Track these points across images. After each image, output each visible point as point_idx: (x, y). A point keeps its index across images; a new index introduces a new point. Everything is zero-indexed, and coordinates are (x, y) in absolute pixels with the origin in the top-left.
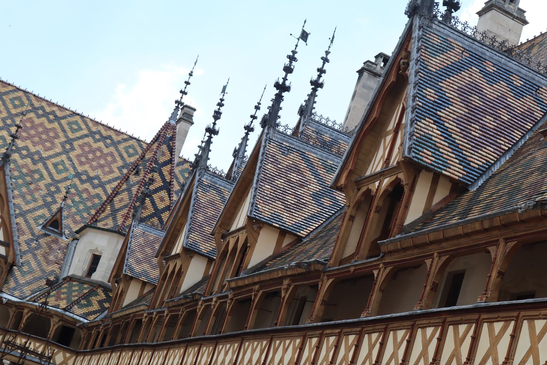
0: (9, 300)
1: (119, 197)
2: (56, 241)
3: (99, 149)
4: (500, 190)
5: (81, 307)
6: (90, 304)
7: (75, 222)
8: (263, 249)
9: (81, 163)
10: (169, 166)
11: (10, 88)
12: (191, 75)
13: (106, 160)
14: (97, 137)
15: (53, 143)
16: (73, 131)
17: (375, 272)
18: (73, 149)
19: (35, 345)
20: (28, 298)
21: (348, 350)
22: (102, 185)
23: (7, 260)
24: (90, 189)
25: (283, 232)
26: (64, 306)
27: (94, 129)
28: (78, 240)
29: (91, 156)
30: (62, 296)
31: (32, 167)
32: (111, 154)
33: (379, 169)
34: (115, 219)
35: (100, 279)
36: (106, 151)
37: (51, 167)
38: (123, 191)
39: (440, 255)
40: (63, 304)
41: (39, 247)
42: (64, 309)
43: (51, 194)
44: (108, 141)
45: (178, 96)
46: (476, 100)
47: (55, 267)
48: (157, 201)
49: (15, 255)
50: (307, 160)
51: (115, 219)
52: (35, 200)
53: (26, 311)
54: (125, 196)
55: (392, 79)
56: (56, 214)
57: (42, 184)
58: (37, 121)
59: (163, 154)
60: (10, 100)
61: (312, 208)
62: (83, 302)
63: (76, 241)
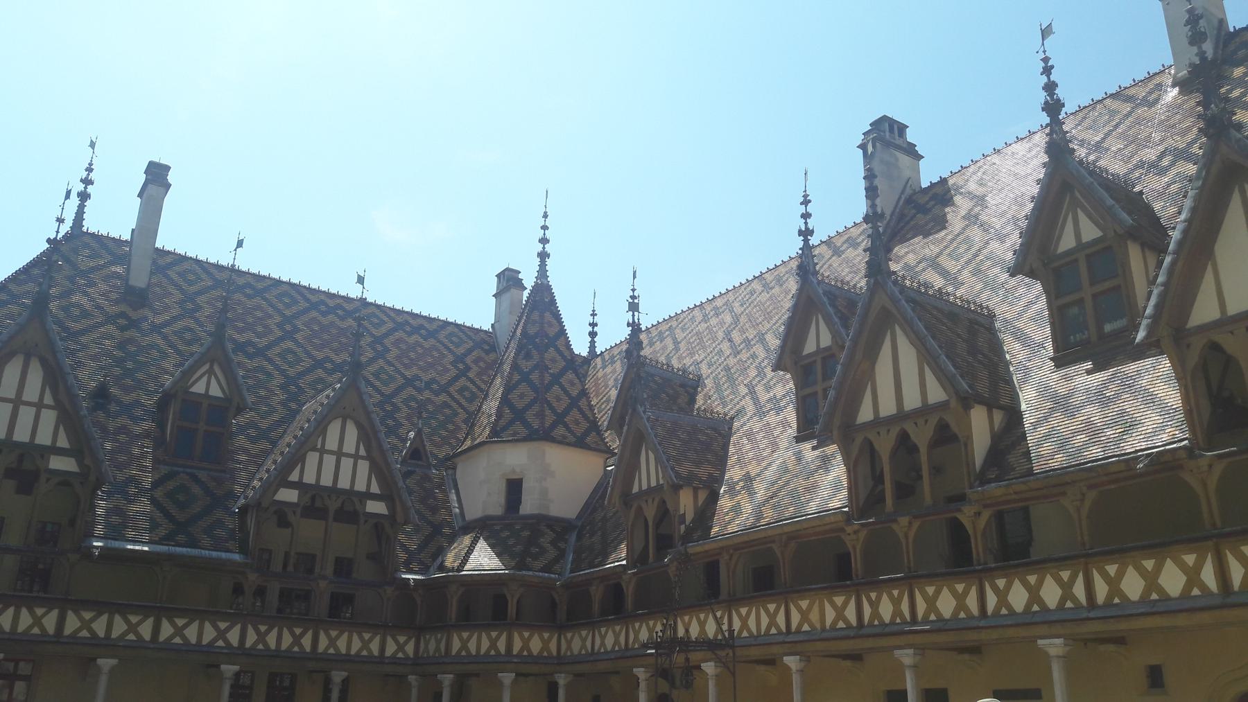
1: (517, 392)
2: (426, 478)
3: (417, 344)
9: (406, 367)
11: (269, 283)
12: (545, 216)
19: (489, 637)
27: (399, 319)
28: (454, 469)
29: (412, 355)
34: (526, 424)
35: (536, 512)
44: (423, 332)
48: (567, 386)
51: (526, 424)
54: (523, 388)
59: (551, 325)
62: (534, 550)
63: (450, 472)
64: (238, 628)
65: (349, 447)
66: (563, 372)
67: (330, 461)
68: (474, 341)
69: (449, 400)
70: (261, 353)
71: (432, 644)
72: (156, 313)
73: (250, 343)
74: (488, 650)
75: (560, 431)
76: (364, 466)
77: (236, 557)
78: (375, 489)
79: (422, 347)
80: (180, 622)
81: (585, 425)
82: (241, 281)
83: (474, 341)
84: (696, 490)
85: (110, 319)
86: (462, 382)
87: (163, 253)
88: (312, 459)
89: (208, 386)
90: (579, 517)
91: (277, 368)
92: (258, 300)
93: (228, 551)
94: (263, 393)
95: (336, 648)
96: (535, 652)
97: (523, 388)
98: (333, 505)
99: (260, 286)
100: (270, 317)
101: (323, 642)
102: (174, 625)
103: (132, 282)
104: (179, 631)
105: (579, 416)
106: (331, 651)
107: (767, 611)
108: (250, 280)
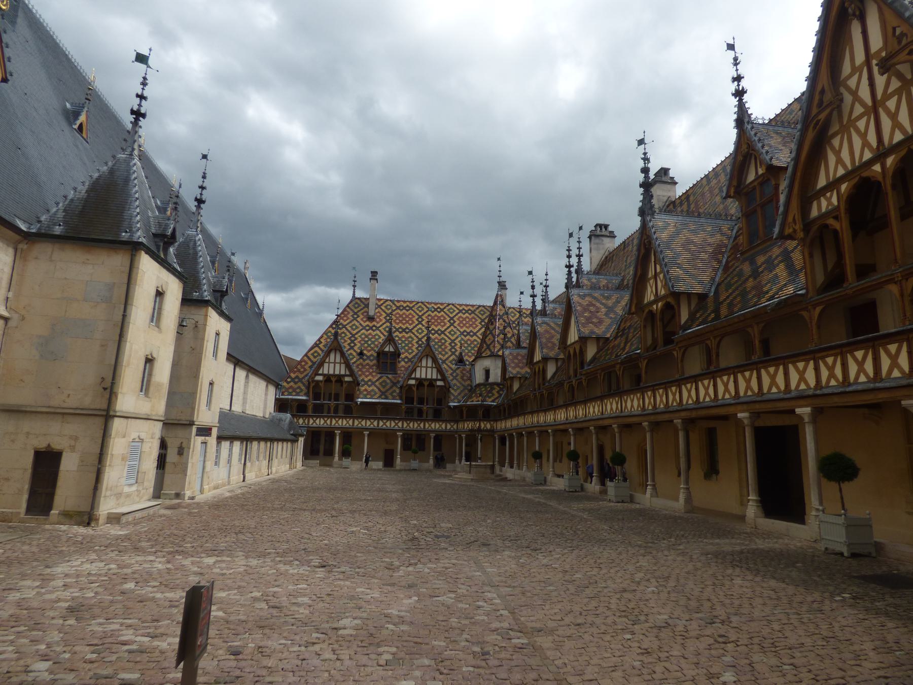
2: (464, 370)
4: (731, 294)
8: (591, 351)
9: (462, 327)
17: (675, 353)
21: (674, 395)
22: (475, 334)
25: (598, 339)
31: (440, 338)
33: (652, 298)
34: (490, 350)
39: (715, 338)
41: (457, 375)
43: (453, 347)
45: (498, 279)
46: (693, 248)
47: (468, 382)
50: (595, 298)
51: (490, 350)
52: (447, 353)
54: (490, 336)
55: (643, 251)
57: (447, 344)
58: (433, 315)
61: (608, 321)
65: (430, 364)
67: (424, 370)
70: (411, 331)
71: (461, 426)
77: (399, 401)
85: (364, 328)
87: (380, 300)
88: (418, 370)
89: (389, 348)
97: (490, 336)
98: (426, 383)
104: (385, 424)
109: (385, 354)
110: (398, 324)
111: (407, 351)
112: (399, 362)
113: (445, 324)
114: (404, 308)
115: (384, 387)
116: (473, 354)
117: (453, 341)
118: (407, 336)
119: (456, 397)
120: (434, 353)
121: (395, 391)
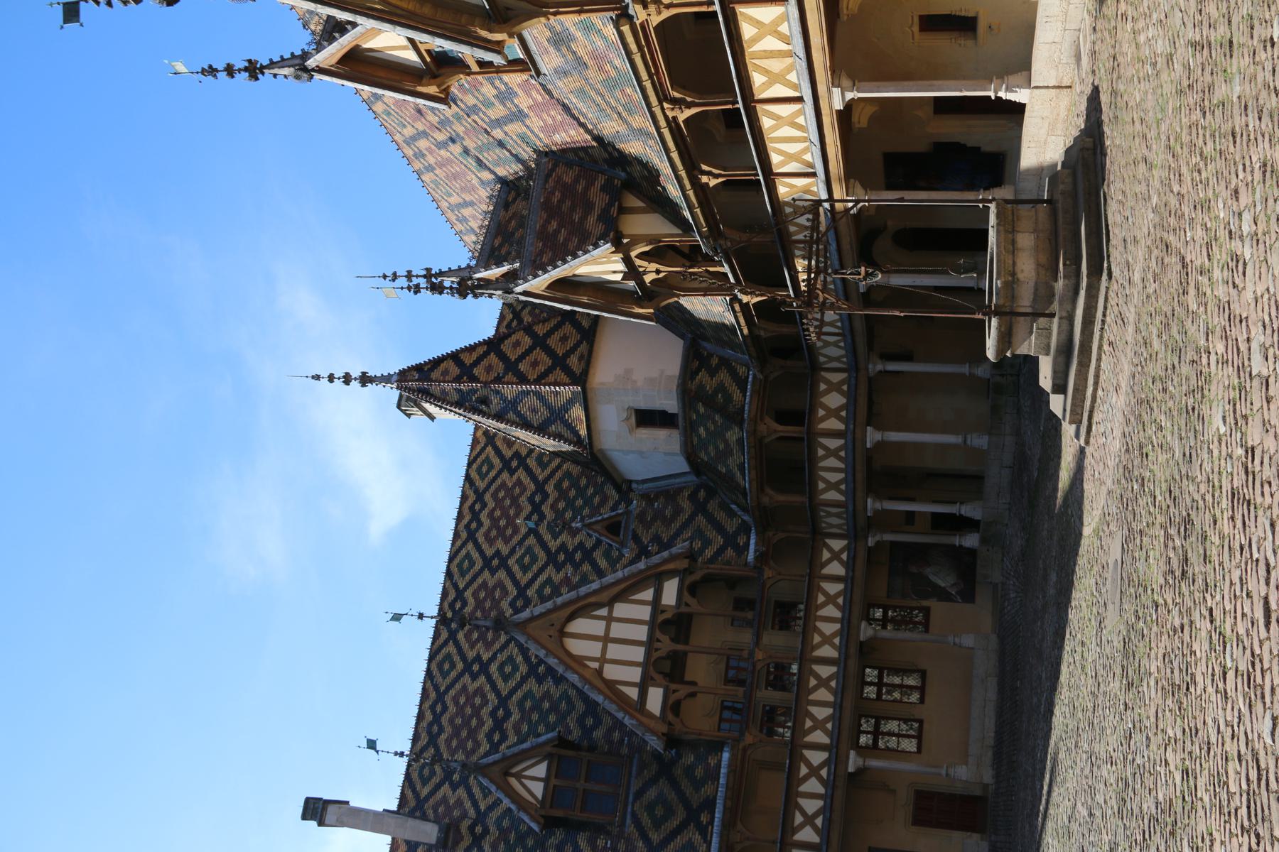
0: (756, 544)
2: (641, 517)
3: (491, 515)
5: (728, 398)
6: (721, 388)
7: (604, 499)
10: (462, 356)
11: (429, 684)
12: (317, 377)
13: (504, 498)
14: (474, 525)
15: (495, 588)
16: (472, 564)
18: (498, 553)
19: (825, 457)
20: (746, 518)
22: (540, 487)
23: (685, 570)
24: (550, 501)
26: (737, 429)
27: (464, 535)
28: (631, 482)
29: (503, 523)
30: (722, 447)
32: (494, 496)
36: (491, 504)
37: (529, 575)
38: (518, 414)
40: (732, 435)
41: (657, 539)
42: (740, 424)
43: (570, 557)
44: (477, 507)
47: (686, 505)
48: (520, 351)
49: (672, 558)
53: (766, 500)
54: (523, 408)
56: (595, 531)
57: (557, 577)
59: (445, 373)
60: (444, 678)
63: (634, 486)
64: (807, 753)
65: (597, 627)
66: (503, 357)
68: (486, 446)
69: (552, 482)
70: (503, 701)
71: (833, 521)
72: (465, 815)
73: (493, 714)
74: (840, 458)
75: (573, 362)
76: (621, 609)
77: (726, 756)
78: (648, 595)
79: (493, 510)
80: (799, 819)
81: (568, 328)
82: (429, 716)
83: (486, 446)
84: (623, 210)
86: (531, 462)
88: (611, 672)
89: (534, 780)
90: (682, 336)
91: (519, 685)
92: (448, 699)
93: (719, 766)
94: (546, 705)
95: (834, 635)
96: (844, 401)
98: (666, 644)
99: (433, 695)
100: (464, 688)
101: (827, 651)
102: (802, 826)
103: (433, 840)
105: (557, 336)
106: (837, 641)
107: (774, 128)
108: (427, 705)
109: (553, 794)
110: (477, 744)
111: (562, 717)
112: (592, 748)
113: (500, 585)
114: (437, 718)
115: (670, 812)
116: (599, 490)
117: (551, 558)
118: (516, 717)
119: (730, 541)
120: (556, 609)
121: (689, 771)
